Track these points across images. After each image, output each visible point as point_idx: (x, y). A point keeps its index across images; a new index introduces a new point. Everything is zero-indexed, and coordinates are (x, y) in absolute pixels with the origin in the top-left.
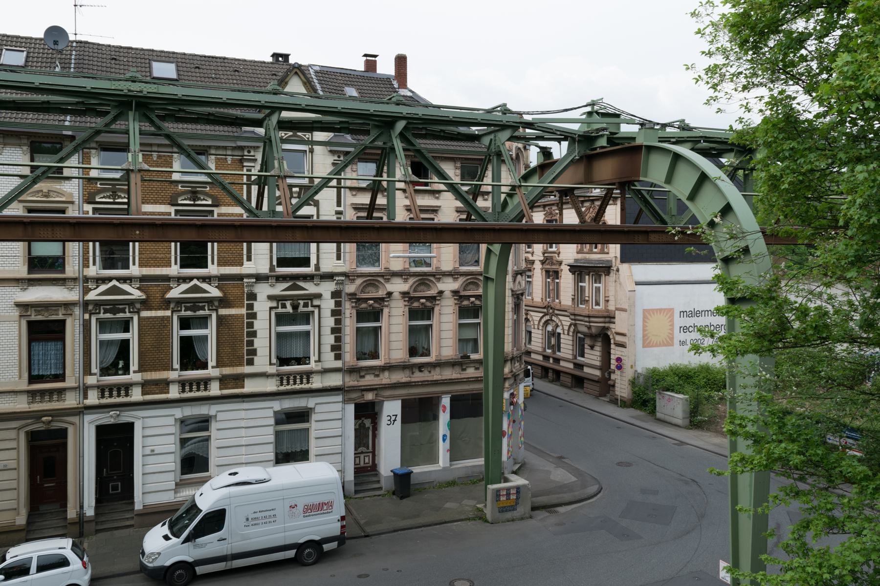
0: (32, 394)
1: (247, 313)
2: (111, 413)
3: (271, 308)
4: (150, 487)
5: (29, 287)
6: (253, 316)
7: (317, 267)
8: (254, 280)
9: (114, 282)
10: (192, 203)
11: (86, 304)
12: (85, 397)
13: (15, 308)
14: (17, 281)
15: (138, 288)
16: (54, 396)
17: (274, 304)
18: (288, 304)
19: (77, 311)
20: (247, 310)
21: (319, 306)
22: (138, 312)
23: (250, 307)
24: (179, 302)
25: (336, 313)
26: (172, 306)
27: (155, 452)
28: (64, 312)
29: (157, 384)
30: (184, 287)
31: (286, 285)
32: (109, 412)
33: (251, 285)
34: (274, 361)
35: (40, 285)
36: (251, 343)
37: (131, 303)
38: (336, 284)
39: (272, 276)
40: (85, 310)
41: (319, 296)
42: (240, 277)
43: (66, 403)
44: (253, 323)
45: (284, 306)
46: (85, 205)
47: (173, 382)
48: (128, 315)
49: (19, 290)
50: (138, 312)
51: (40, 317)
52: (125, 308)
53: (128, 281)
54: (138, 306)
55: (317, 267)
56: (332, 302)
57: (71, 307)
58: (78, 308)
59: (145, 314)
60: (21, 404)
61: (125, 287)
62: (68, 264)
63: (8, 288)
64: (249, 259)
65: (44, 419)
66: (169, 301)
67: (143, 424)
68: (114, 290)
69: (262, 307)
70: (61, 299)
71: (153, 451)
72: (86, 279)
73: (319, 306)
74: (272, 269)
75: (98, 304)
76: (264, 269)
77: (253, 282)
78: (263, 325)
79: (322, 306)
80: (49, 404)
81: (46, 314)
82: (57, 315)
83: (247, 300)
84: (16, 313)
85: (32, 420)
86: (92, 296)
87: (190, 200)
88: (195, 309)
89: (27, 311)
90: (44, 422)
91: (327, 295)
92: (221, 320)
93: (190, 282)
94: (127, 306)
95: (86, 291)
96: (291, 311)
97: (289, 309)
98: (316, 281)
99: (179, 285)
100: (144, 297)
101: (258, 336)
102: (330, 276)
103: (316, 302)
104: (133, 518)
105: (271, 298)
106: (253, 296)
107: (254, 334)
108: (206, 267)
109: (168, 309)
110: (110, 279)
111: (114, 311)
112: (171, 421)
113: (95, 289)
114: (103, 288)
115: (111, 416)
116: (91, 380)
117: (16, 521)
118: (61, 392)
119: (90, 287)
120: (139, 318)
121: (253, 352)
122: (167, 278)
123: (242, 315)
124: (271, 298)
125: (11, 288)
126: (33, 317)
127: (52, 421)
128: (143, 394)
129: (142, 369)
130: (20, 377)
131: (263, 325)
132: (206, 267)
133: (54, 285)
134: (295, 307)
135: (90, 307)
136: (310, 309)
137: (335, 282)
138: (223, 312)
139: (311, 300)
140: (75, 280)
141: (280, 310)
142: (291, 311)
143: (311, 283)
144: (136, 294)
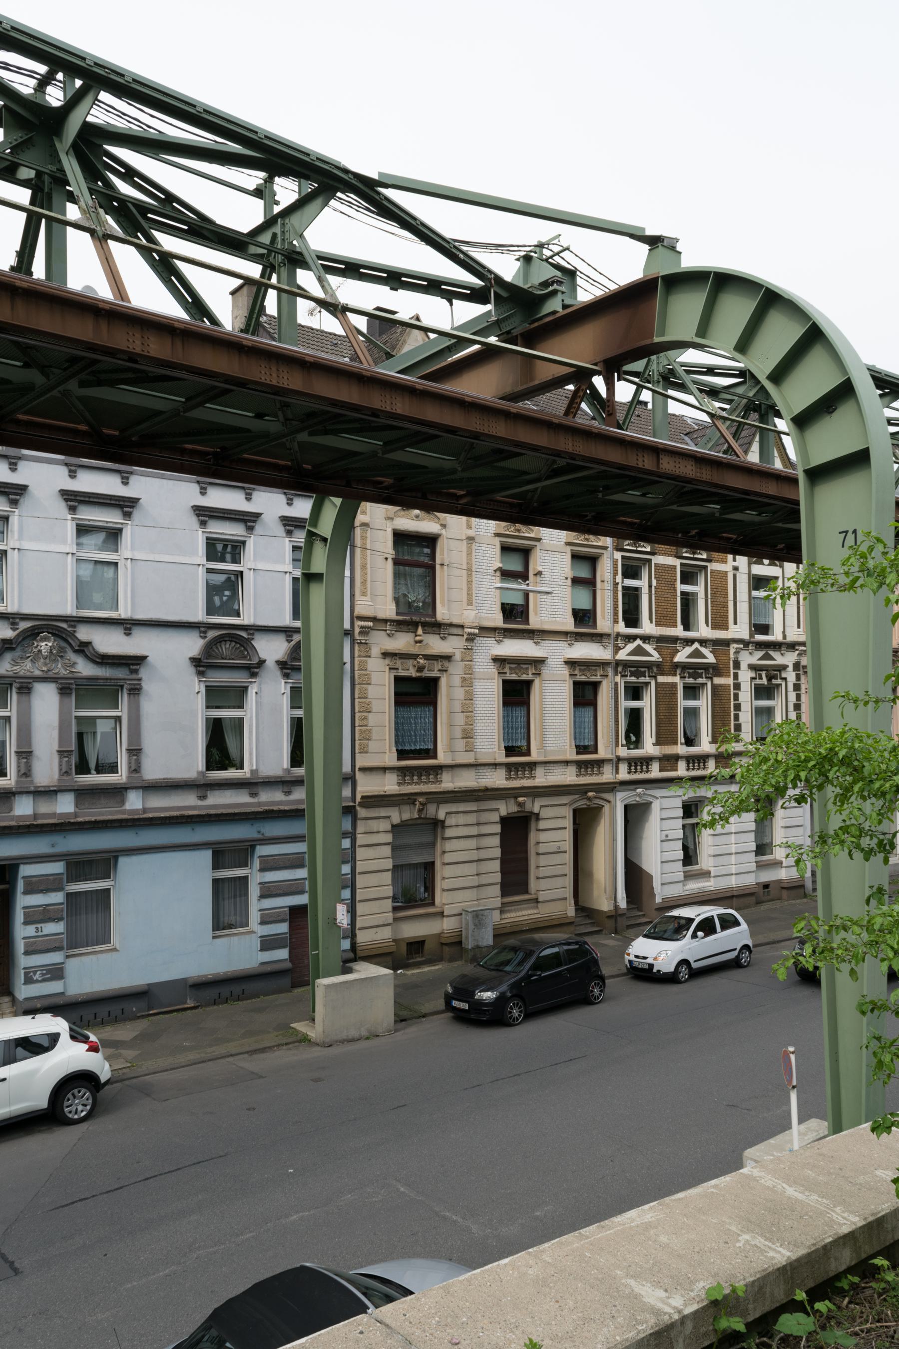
0: (580, 764)
1: (734, 684)
2: (639, 790)
3: (753, 679)
4: (668, 878)
5: (575, 643)
6: (737, 686)
7: (784, 637)
8: (742, 646)
9: (638, 642)
10: (692, 556)
11: (618, 663)
12: (617, 773)
13: (564, 666)
14: (566, 634)
15: (655, 649)
16: (595, 769)
17: (754, 675)
18: (764, 674)
19: (610, 671)
20: (734, 680)
21: (785, 679)
22: (655, 677)
23: (736, 676)
24: (684, 667)
25: (797, 687)
26: (678, 672)
27: (670, 838)
28: (602, 673)
29: (668, 760)
30: (689, 650)
31: (760, 654)
32: (635, 790)
33: (737, 652)
34: (755, 739)
35: (583, 641)
36: (737, 717)
37: (649, 665)
38: (799, 654)
39: (753, 643)
40: (616, 674)
41: (784, 667)
42: (726, 643)
43: (605, 776)
44: (738, 694)
45: (761, 678)
46: (615, 552)
47: (682, 757)
48: (647, 679)
49: (567, 645)
50: (655, 677)
51: (584, 677)
52: (645, 671)
53: (647, 641)
54: (655, 669)
55: (784, 637)
56: (794, 674)
57: (606, 667)
58: (610, 669)
59: (661, 679)
60: (568, 776)
61: (648, 648)
62: (604, 618)
63: (558, 642)
64: (735, 623)
65: (590, 794)
66: (677, 665)
67: (661, 803)
68: (639, 651)
69: (745, 676)
70: (599, 658)
71: (667, 836)
72: (618, 635)
73: (785, 679)
74: (752, 636)
75: (626, 664)
76: (745, 635)
77: (741, 649)
78: (746, 696)
79: (788, 680)
80: (591, 778)
81: (588, 674)
82: (596, 676)
83: (734, 669)
84: (565, 672)
85: (577, 796)
86: (622, 655)
87: (690, 554)
88: (695, 676)
89: (574, 670)
90: (589, 799)
91: (791, 668)
92: (715, 688)
93: (691, 645)
94: (647, 669)
95: (617, 649)
96: (766, 683)
97: (764, 681)
98: (783, 649)
99: (684, 648)
100: (661, 660)
101: (742, 709)
102: (792, 646)
103: (784, 675)
104: (644, 915)
105: (752, 667)
106: (737, 665)
107: (738, 707)
108: (727, 629)
109: (675, 675)
110: (633, 638)
111: (637, 674)
112: (678, 803)
113: (624, 648)
114: (631, 647)
115: (639, 795)
116: (623, 752)
117: (568, 912)
118: (600, 763)
119: (620, 645)
120: (656, 683)
121: (738, 728)
122: (675, 640)
123: (729, 686)
124: (752, 667)
125: (561, 642)
126: (578, 677)
127: (595, 797)
128: (661, 770)
129: (658, 743)
130: (570, 746)
131: (746, 696)
132: (727, 629)
133: (593, 641)
134: (770, 679)
135: (620, 669)
136: (779, 681)
137: (797, 652)
138: (718, 681)
139: (780, 671)
140: (609, 635)
141: (758, 681)
142: (766, 683)
143: (779, 653)
144: (655, 656)
